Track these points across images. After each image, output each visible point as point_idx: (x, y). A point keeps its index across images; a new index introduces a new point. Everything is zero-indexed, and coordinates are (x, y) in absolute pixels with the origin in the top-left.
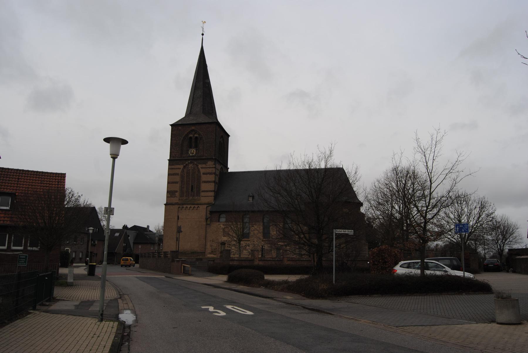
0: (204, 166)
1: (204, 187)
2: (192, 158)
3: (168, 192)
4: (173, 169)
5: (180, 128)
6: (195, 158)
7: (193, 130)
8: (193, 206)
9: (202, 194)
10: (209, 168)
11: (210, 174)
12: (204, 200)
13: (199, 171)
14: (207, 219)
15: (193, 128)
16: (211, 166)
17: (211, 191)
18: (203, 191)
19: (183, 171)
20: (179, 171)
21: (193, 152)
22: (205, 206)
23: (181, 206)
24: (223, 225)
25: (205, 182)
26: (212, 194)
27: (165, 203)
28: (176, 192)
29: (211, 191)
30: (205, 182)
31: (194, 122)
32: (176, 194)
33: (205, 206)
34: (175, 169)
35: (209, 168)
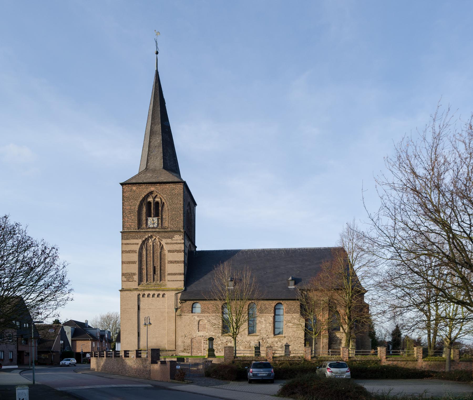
0: (169, 241)
1: (169, 268)
2: (154, 230)
3: (123, 275)
4: (128, 244)
5: (134, 188)
6: (157, 230)
7: (151, 193)
8: (156, 293)
9: (168, 278)
10: (176, 243)
11: (178, 251)
12: (170, 285)
13: (162, 248)
14: (177, 309)
15: (152, 188)
16: (179, 242)
17: (180, 274)
18: (169, 274)
19: (141, 248)
20: (137, 248)
21: (152, 221)
22: (174, 293)
23: (141, 293)
24: (198, 316)
25: (171, 262)
26: (182, 277)
27: (120, 289)
28: (134, 274)
29: (180, 274)
30: (171, 262)
31: (154, 180)
32: (134, 277)
33: (174, 293)
34: (131, 244)
35: (176, 243)
